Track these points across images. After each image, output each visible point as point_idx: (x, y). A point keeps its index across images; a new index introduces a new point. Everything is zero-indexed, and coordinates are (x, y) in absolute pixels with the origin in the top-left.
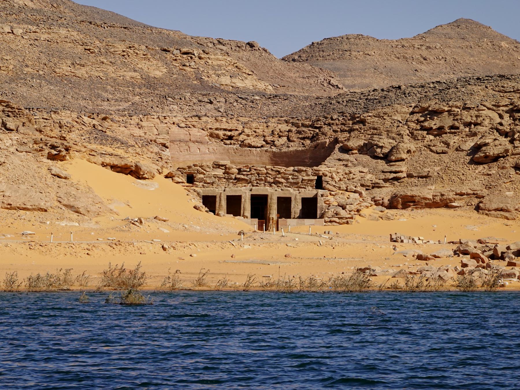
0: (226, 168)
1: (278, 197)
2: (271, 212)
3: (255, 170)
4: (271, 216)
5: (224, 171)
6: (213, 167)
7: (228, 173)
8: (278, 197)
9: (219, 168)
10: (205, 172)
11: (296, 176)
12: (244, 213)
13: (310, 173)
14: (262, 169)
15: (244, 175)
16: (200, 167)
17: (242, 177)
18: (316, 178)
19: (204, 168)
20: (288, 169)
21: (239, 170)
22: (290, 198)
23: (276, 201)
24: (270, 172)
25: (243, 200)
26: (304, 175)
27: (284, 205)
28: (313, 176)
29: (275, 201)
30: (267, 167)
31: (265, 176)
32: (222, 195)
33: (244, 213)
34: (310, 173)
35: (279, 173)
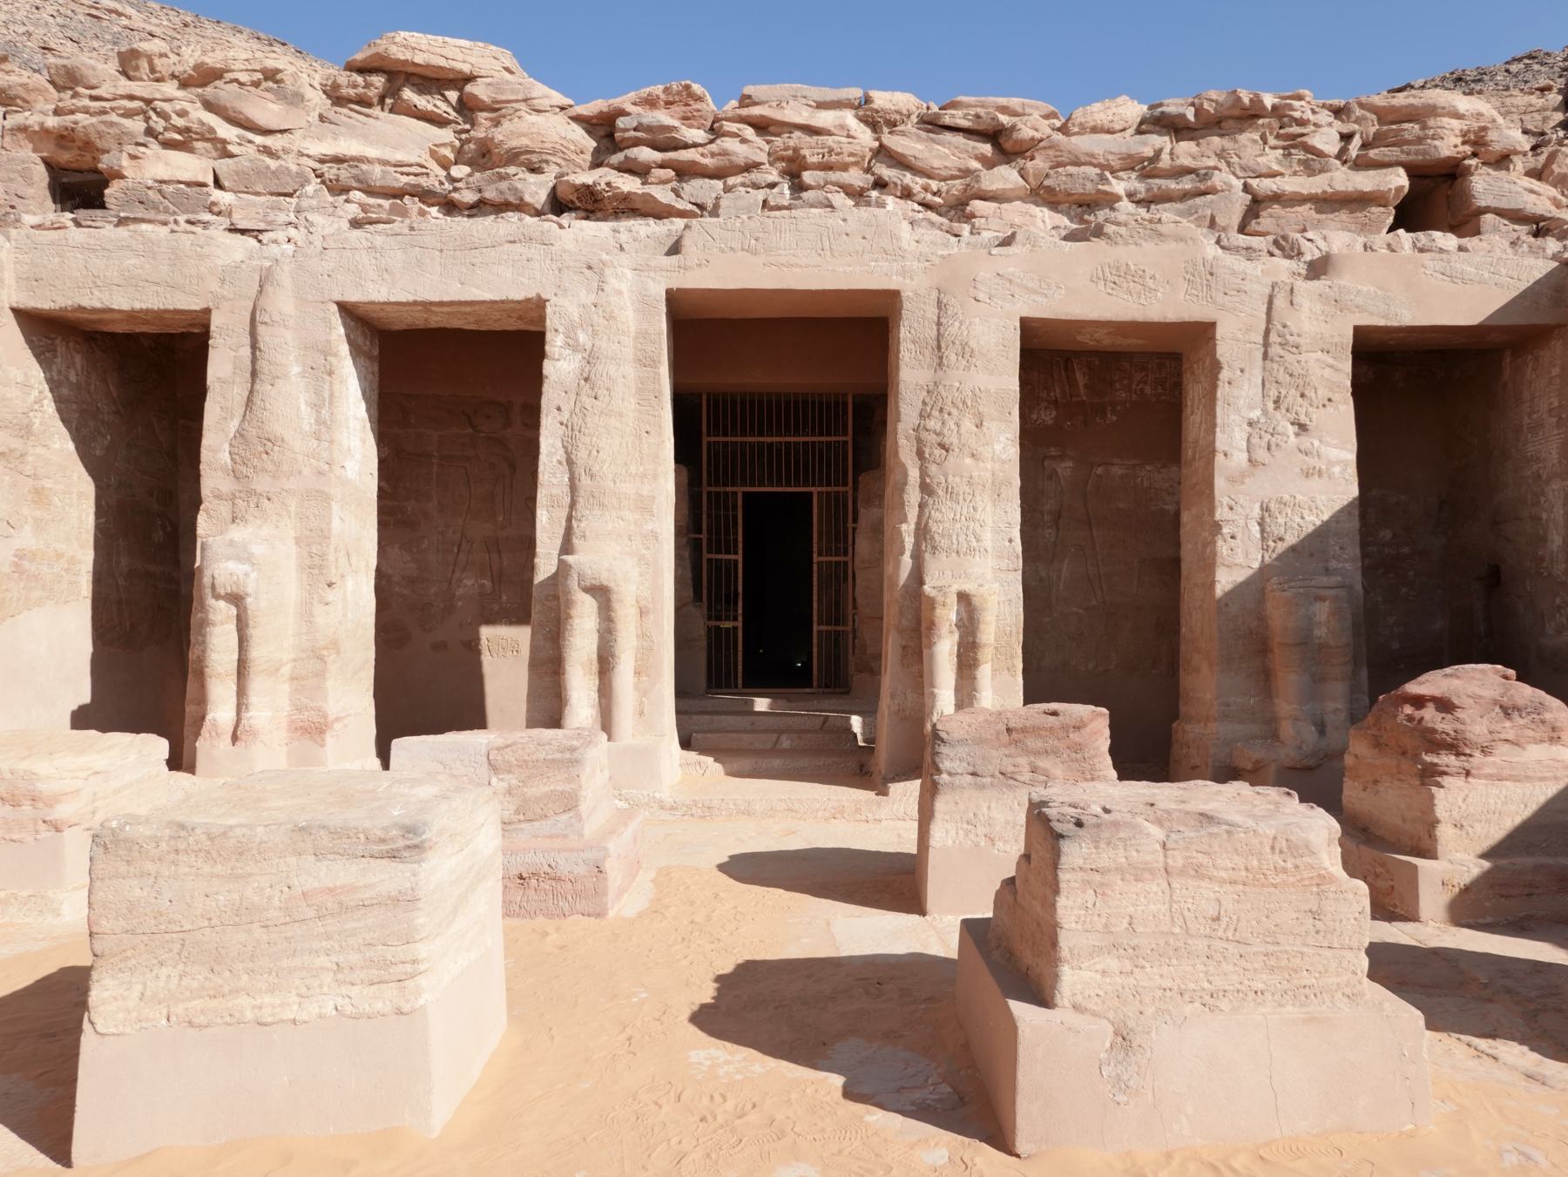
0: (467, 108)
1: (1023, 321)
2: (944, 517)
3: (763, 127)
4: (942, 581)
5: (447, 135)
6: (337, 98)
7: (484, 157)
8: (1029, 329)
9: (389, 99)
10: (225, 131)
11: (1180, 172)
12: (567, 547)
13: (1326, 139)
14: (825, 119)
15: (640, 171)
16: (184, 84)
17: (629, 184)
18: (1399, 180)
19: (222, 92)
20: (1098, 112)
21: (605, 130)
22: (1203, 333)
23: (1011, 383)
24: (909, 143)
25: (559, 367)
26: (1272, 158)
27: (1065, 468)
28: (1361, 164)
29: (997, 378)
30: (883, 100)
31: (855, 177)
32: (282, 303)
33: (567, 547)
34: (1326, 139)
35: (1000, 141)
